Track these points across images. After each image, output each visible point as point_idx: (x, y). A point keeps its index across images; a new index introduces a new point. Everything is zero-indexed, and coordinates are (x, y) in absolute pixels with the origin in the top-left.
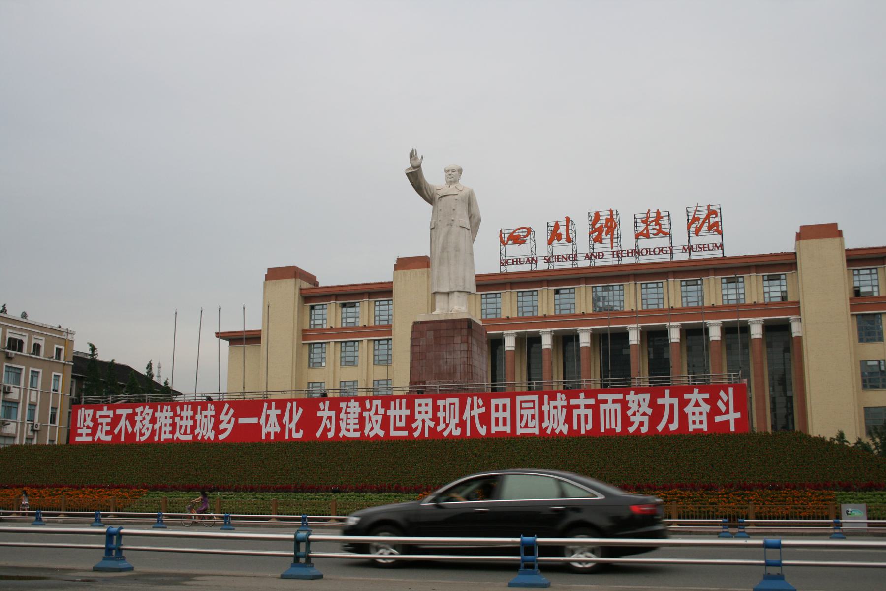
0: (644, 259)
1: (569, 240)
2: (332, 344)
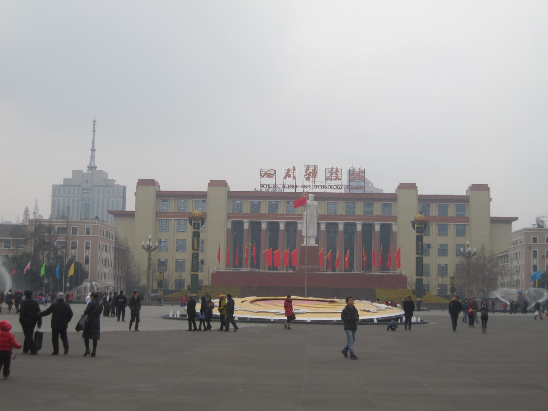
0: (328, 191)
1: (294, 178)
2: (173, 221)
